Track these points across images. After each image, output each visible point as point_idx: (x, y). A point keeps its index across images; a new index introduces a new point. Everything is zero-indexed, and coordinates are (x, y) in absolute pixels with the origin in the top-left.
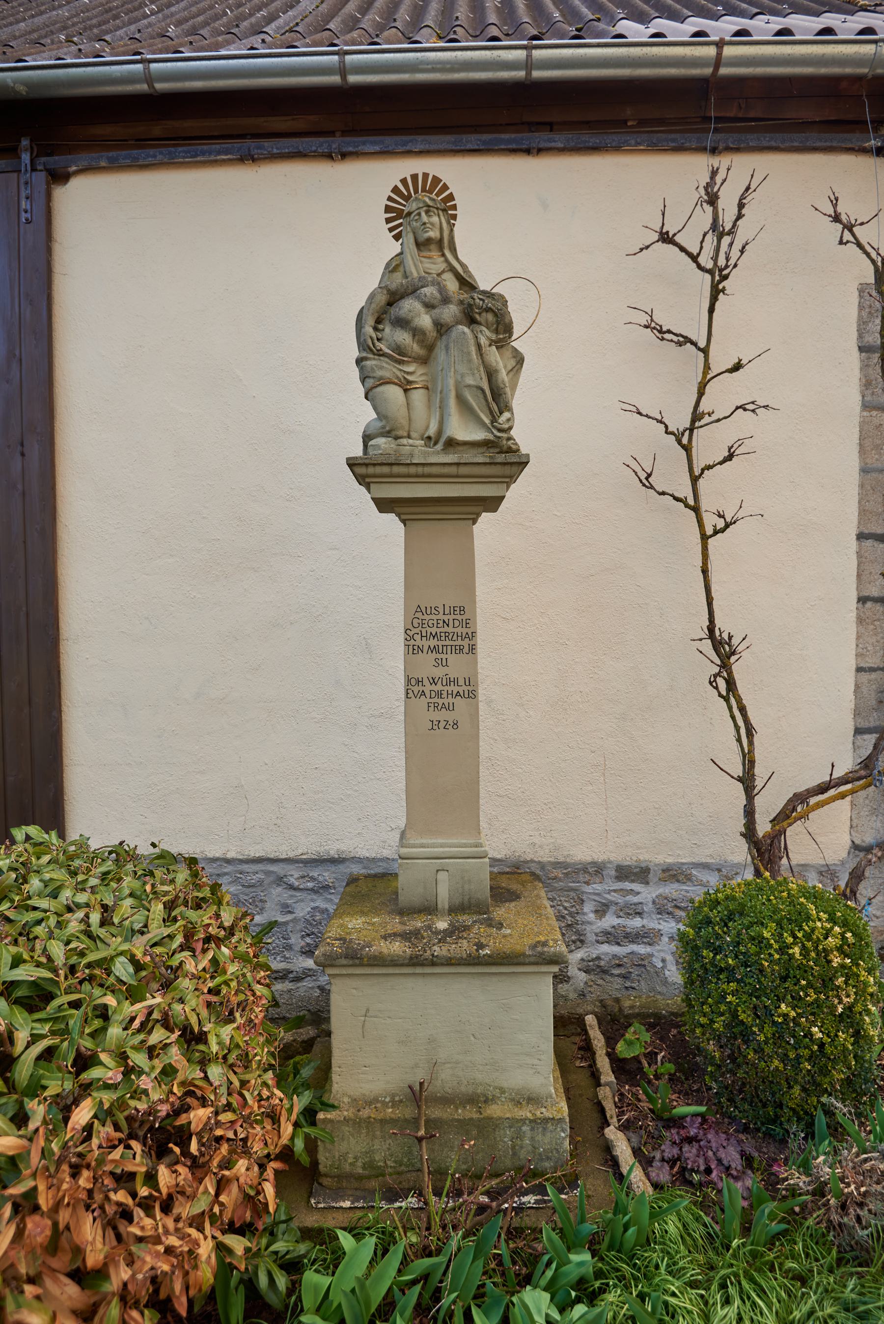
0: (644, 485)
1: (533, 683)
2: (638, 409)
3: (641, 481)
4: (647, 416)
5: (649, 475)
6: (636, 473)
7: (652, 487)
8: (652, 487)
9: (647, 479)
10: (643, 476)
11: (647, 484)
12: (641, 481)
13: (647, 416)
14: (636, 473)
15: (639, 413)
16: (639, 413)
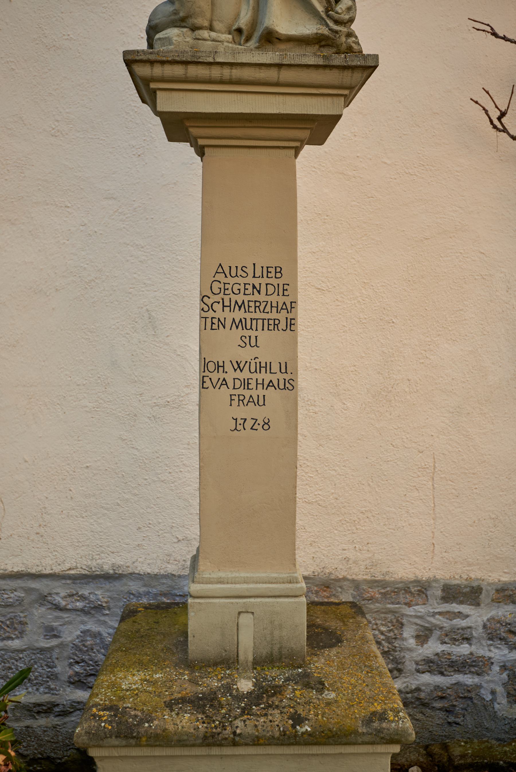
0: (495, 127)
1: (352, 368)
2: (492, 29)
3: (491, 122)
4: (504, 38)
5: (503, 114)
6: (486, 112)
7: (505, 130)
8: (505, 130)
9: (499, 119)
10: (495, 114)
11: (499, 126)
12: (491, 122)
13: (504, 38)
14: (486, 112)
15: (495, 34)
16: (495, 34)
